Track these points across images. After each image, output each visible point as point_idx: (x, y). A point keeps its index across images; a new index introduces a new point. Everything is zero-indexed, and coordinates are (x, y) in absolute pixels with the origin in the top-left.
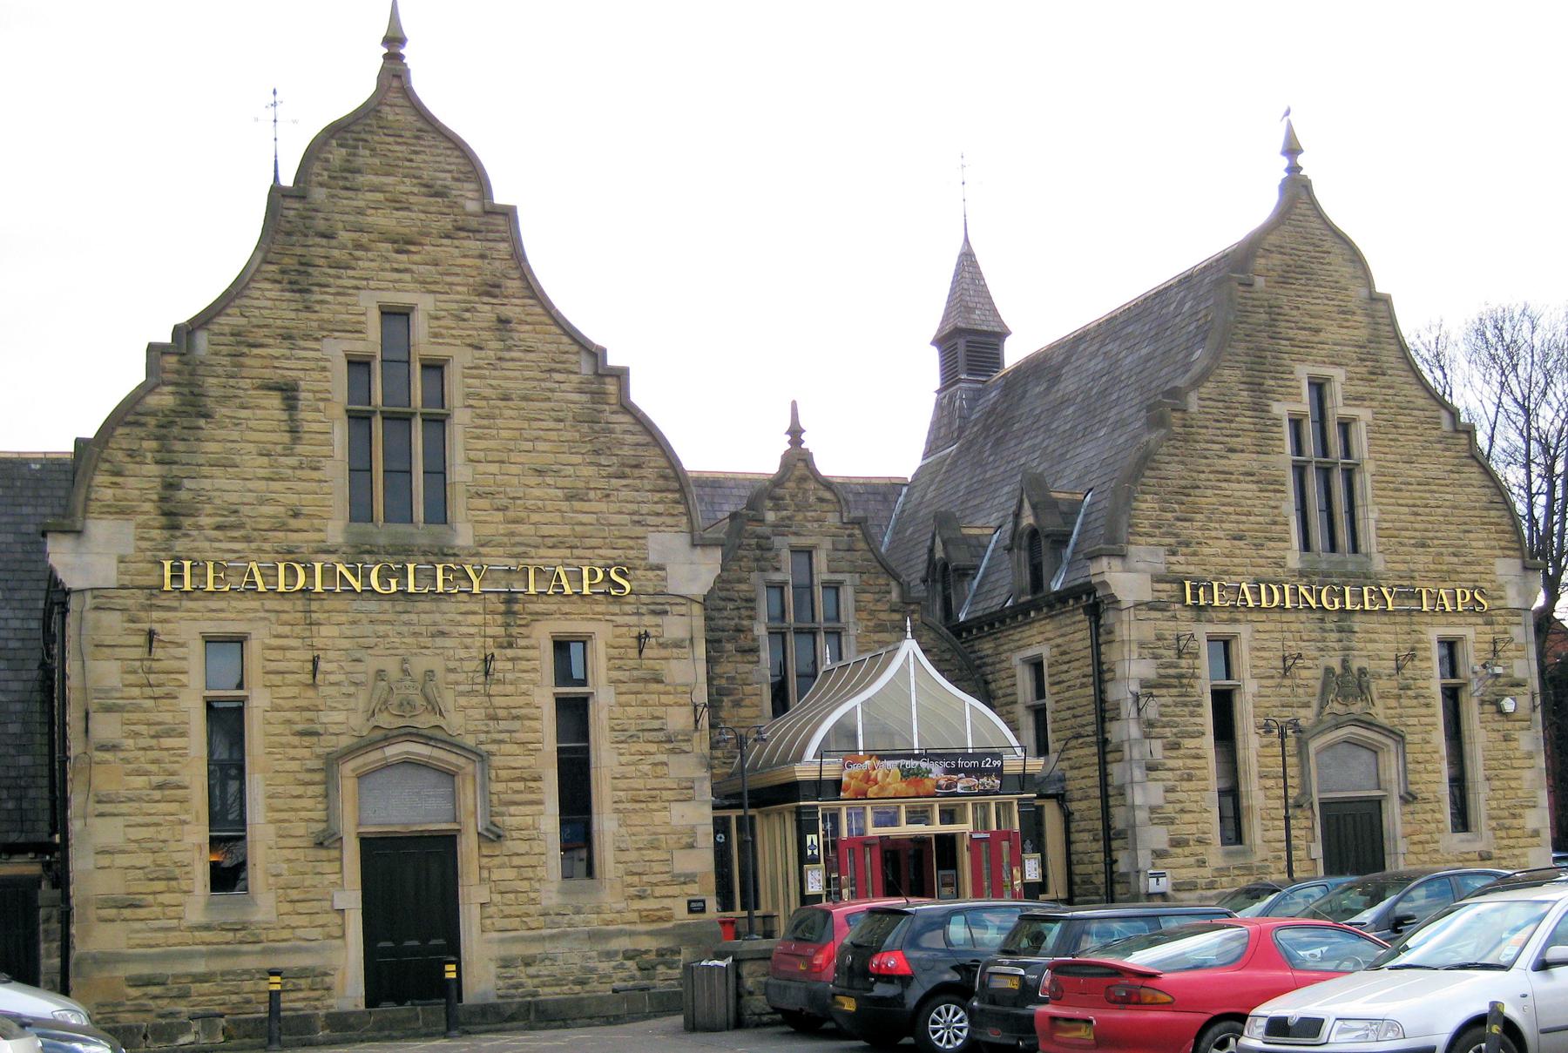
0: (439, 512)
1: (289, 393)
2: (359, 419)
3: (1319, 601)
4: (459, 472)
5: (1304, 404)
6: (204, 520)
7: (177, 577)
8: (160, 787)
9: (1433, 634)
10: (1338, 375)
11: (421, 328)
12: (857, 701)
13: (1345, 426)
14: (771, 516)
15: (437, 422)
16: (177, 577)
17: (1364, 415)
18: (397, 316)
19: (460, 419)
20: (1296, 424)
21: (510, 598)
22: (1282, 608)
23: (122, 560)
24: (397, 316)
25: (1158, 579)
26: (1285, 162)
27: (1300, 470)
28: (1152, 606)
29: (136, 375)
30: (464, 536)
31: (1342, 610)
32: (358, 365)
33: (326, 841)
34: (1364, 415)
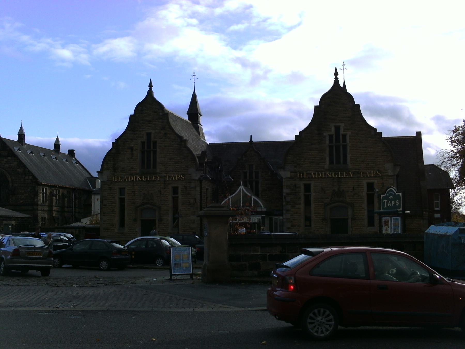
0: (155, 167)
1: (132, 149)
2: (143, 153)
3: (332, 175)
4: (158, 160)
5: (333, 132)
6: (119, 170)
7: (115, 179)
8: (112, 211)
9: (364, 182)
10: (342, 125)
11: (152, 136)
12: (230, 197)
13: (344, 136)
14: (244, 159)
15: (155, 153)
16: (115, 179)
17: (349, 133)
18: (149, 135)
19: (158, 151)
20: (331, 137)
21: (165, 181)
22: (321, 177)
23: (108, 177)
24: (149, 135)
25: (291, 172)
26: (334, 77)
27: (331, 147)
28: (289, 178)
29: (111, 147)
30: (158, 171)
31: (338, 177)
32: (143, 143)
33: (135, 220)
34: (349, 133)
